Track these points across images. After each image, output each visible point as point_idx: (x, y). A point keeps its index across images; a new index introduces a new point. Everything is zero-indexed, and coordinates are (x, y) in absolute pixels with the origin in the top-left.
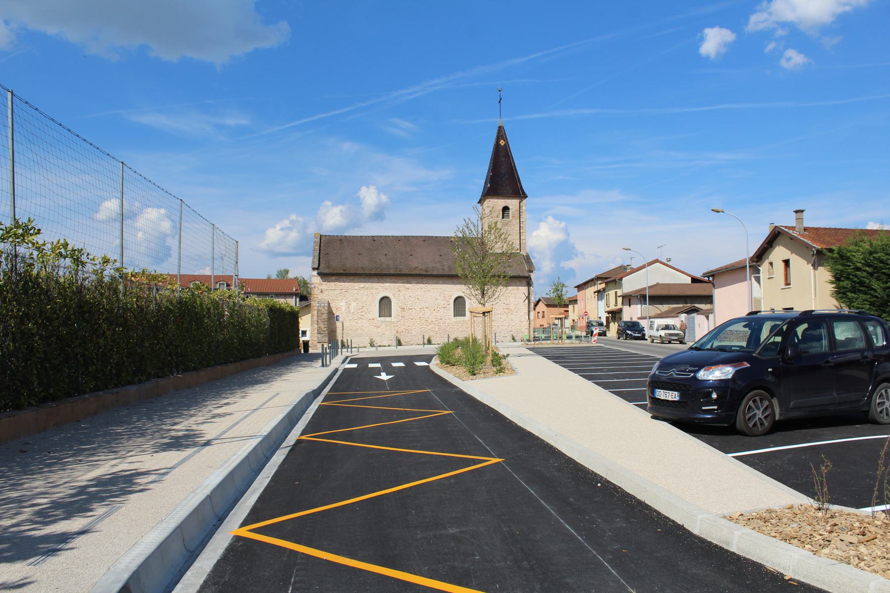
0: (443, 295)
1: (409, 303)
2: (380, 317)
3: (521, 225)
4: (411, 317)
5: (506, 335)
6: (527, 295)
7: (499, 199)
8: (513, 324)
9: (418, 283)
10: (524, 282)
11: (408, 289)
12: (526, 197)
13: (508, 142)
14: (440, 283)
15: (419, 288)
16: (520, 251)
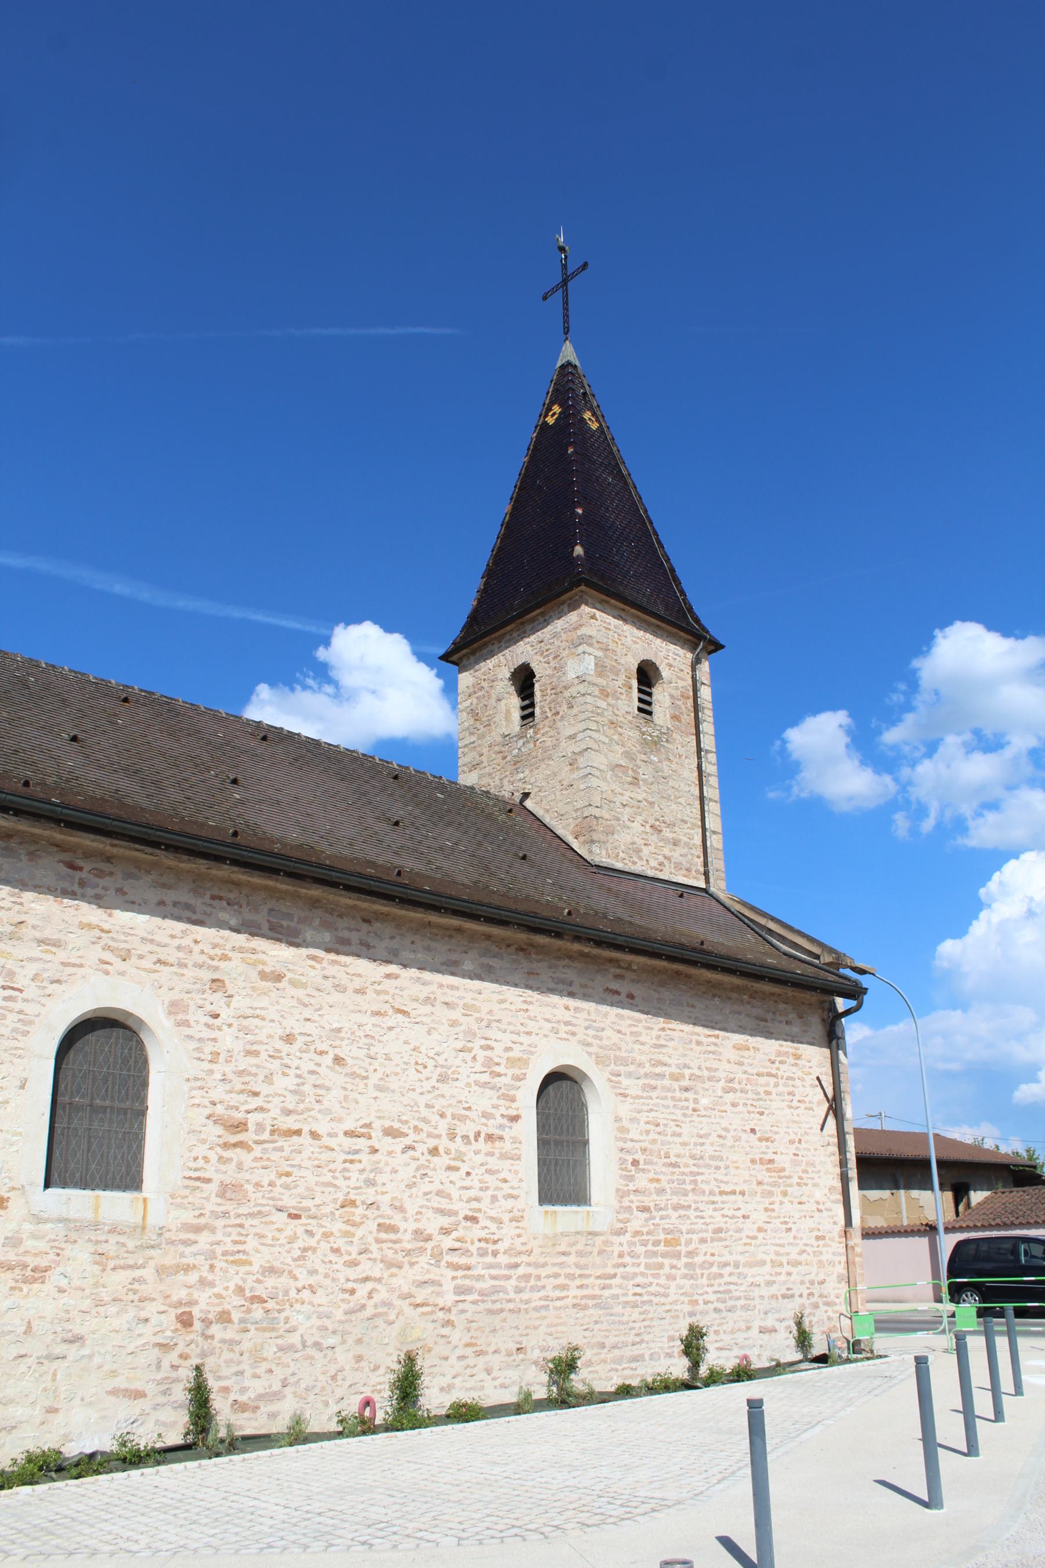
0: (481, 1054)
1: (282, 1083)
2: (47, 1185)
4: (289, 1201)
5: (770, 1322)
8: (794, 1252)
9: (340, 946)
11: (278, 978)
14: (468, 966)
15: (344, 979)
16: (707, 881)
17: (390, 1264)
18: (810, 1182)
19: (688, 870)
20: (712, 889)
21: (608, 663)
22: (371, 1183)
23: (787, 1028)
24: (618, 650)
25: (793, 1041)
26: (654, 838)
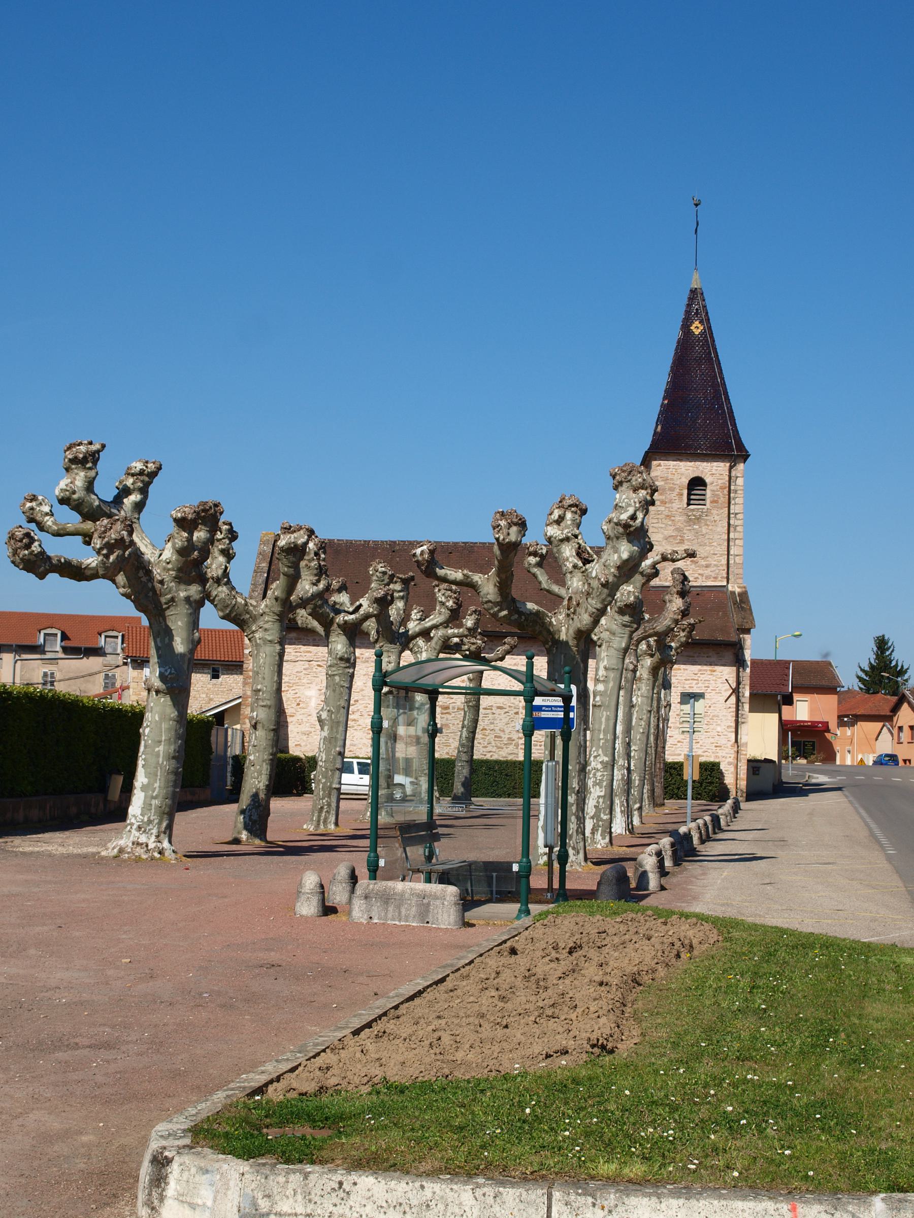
3: (732, 522)
6: (734, 687)
7: (681, 460)
10: (729, 655)
12: (744, 456)
13: (710, 328)
16: (728, 582)
17: (498, 748)
18: (715, 724)
19: (715, 578)
20: (730, 588)
21: (667, 487)
22: (492, 723)
23: (708, 659)
24: (675, 477)
25: (711, 665)
26: (693, 566)
